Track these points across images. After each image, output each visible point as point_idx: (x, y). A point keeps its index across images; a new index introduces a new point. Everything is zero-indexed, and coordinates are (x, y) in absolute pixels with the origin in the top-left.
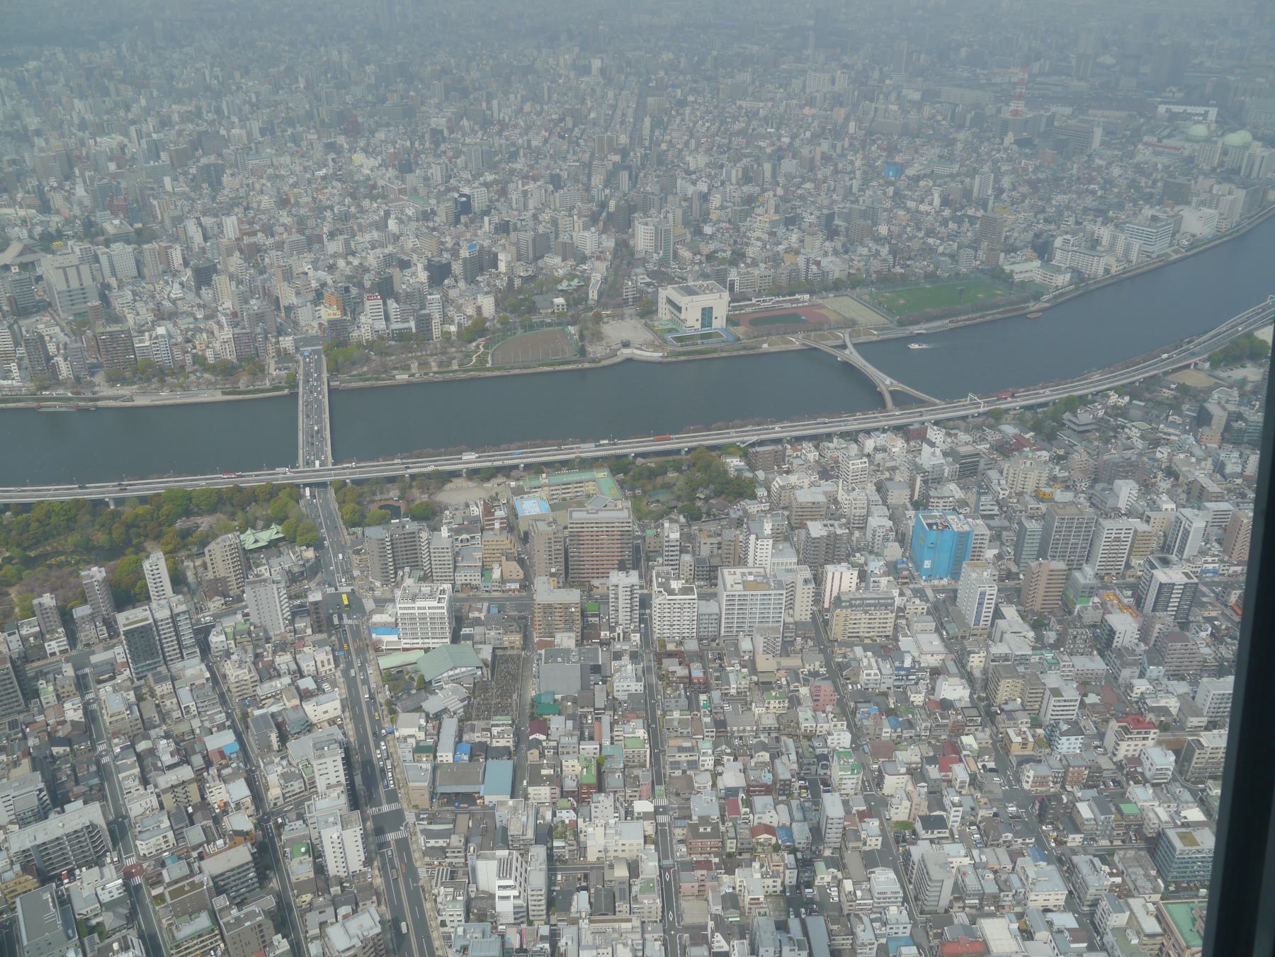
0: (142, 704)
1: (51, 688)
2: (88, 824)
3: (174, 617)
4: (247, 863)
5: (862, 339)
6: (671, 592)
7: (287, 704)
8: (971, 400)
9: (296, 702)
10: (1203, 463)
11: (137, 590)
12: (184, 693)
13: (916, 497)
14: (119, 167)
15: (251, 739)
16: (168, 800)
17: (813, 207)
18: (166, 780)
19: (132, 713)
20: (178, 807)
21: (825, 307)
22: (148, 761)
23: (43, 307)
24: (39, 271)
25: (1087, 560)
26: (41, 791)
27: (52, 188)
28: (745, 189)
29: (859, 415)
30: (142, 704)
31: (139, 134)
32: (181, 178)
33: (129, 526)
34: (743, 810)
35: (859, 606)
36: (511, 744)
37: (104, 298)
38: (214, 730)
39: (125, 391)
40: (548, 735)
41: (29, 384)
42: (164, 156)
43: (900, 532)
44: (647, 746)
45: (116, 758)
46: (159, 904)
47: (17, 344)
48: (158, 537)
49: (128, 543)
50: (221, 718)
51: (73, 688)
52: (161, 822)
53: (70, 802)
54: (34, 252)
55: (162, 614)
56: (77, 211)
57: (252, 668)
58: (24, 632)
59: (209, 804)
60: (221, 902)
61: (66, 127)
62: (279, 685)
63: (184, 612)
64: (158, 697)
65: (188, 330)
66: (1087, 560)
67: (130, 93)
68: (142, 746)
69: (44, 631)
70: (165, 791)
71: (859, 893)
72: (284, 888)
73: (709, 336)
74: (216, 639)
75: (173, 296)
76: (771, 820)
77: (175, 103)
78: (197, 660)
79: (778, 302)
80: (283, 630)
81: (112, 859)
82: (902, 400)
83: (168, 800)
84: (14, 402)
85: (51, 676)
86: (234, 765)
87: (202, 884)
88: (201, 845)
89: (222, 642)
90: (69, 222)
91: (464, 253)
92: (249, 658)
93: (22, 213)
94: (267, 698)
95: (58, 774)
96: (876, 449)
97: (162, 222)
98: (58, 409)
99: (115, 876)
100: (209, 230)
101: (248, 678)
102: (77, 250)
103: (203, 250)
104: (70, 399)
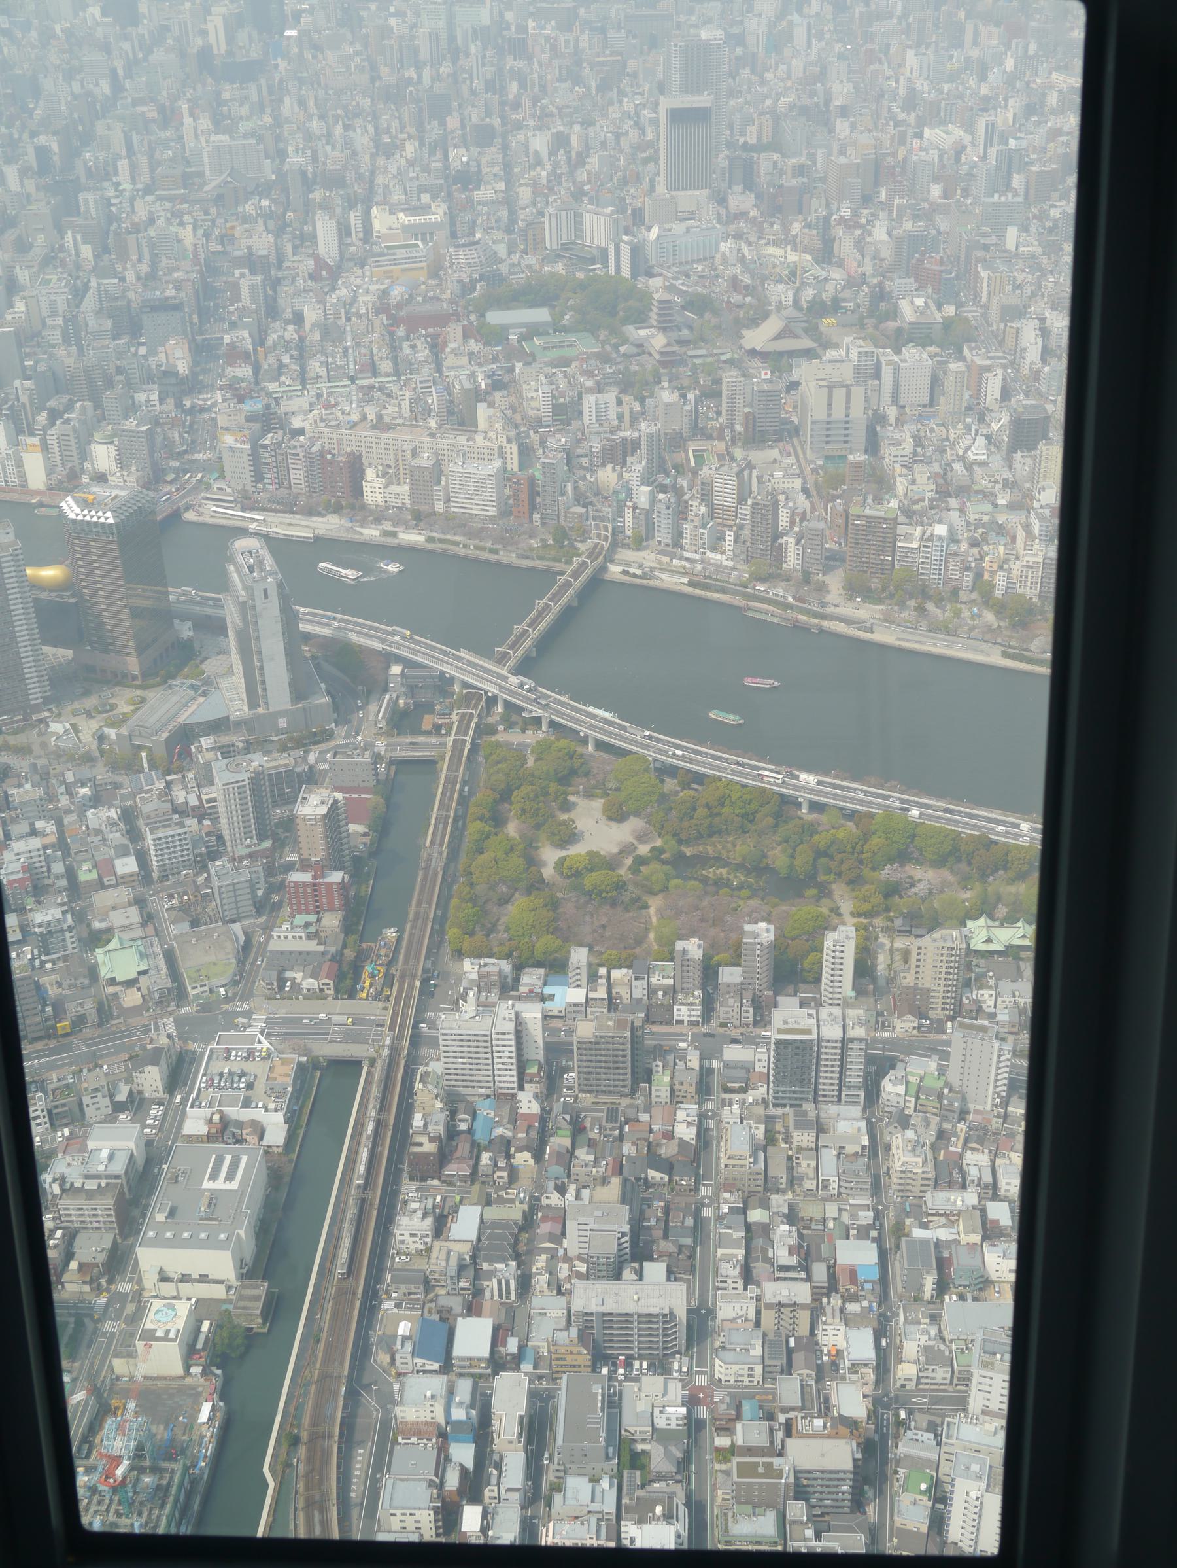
0: (770, 1149)
1: (667, 1079)
2: (667, 1311)
3: (845, 1042)
4: (845, 1472)
7: (962, 1235)
9: (976, 1238)
11: (806, 964)
12: (828, 1157)
14: (946, 195)
15: (897, 1263)
16: (769, 1319)
18: (776, 1292)
19: (755, 1162)
20: (778, 1333)
22: (758, 1242)
23: (786, 433)
24: (795, 375)
26: (623, 1234)
27: (842, 220)
30: (770, 1149)
31: (990, 127)
32: (1034, 226)
33: (820, 853)
37: (873, 445)
38: (853, 1232)
39: (865, 612)
41: (742, 566)
42: (1017, 181)
45: (720, 1218)
46: (719, 1462)
47: (741, 500)
48: (855, 882)
49: (810, 879)
50: (867, 1217)
51: (693, 1089)
52: (753, 1346)
53: (651, 1259)
54: (796, 336)
55: (832, 1032)
56: (868, 268)
57: (930, 1157)
58: (654, 980)
59: (817, 1343)
60: (797, 1510)
61: (885, 103)
62: (959, 1203)
63: (861, 1040)
64: (794, 1146)
65: (979, 524)
67: (994, 42)
68: (756, 1215)
69: (678, 987)
70: (769, 1306)
72: (882, 1524)
74: (892, 1088)
75: (971, 456)
77: (1058, 69)
78: (856, 1111)
80: (988, 1108)
81: (680, 1367)
83: (769, 1319)
84: (717, 591)
85: (670, 1058)
86: (865, 1304)
87: (779, 1474)
88: (793, 1409)
89: (899, 1095)
90: (855, 282)
92: (930, 1136)
93: (793, 257)
94: (937, 1214)
95: (648, 1213)
97: (986, 307)
98: (769, 618)
99: (679, 1401)
100: (1053, 336)
101: (920, 1171)
102: (854, 355)
103: (1036, 376)
104: (790, 607)
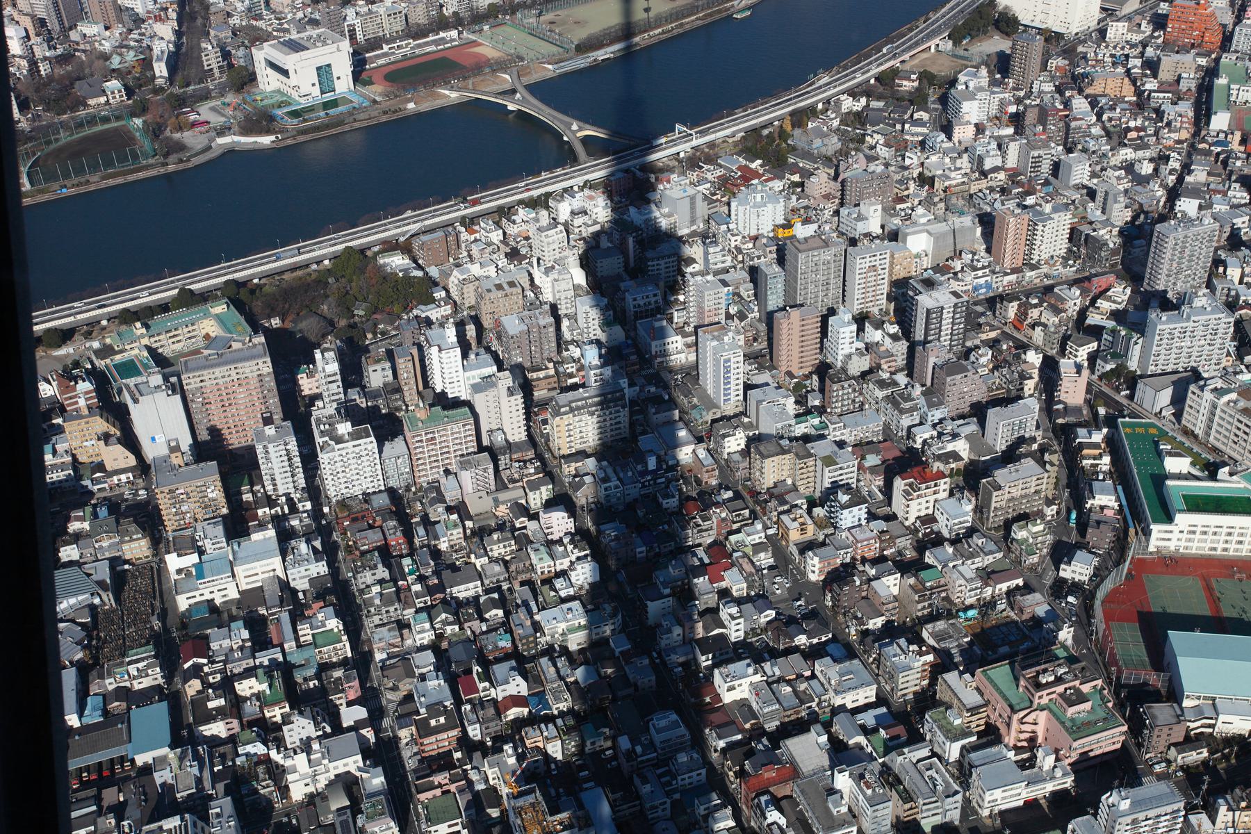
6: (339, 440)
10: (958, 163)
13: (632, 264)
21: (480, 44)
25: (844, 301)
29: (544, 175)
34: (481, 686)
35: (583, 408)
36: (161, 681)
40: (209, 657)
43: (618, 309)
44: (345, 638)
66: (844, 301)
71: (639, 749)
73: (333, 103)
76: (518, 689)
79: (419, 46)
96: (573, 213)
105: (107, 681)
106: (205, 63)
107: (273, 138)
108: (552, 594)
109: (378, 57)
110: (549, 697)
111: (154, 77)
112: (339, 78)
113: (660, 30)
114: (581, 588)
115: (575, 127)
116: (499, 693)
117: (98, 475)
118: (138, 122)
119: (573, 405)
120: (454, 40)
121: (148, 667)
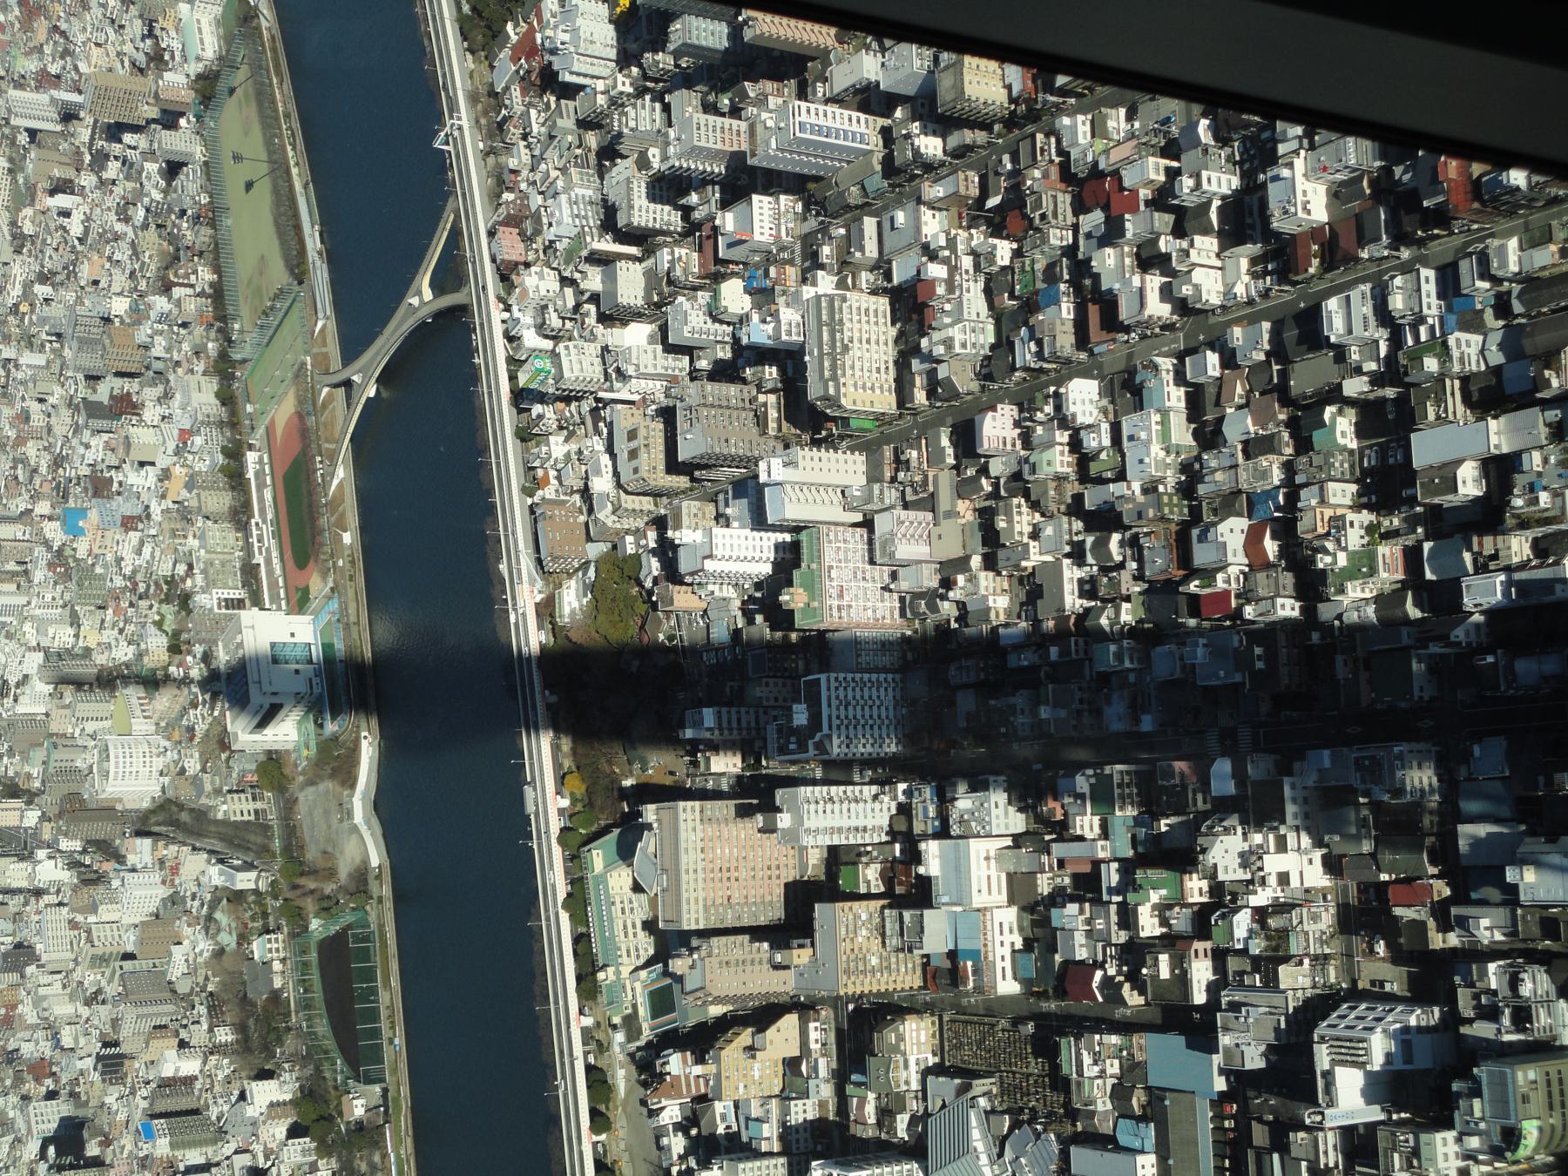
5: (333, 349)
8: (447, 143)
17: (75, 442)
28: (39, 575)
35: (834, 361)
82: (451, 274)
91: (162, 1147)
105: (1100, 1107)
106: (246, 818)
107: (364, 744)
108: (1103, 456)
109: (270, 572)
110: (1260, 487)
111: (256, 892)
112: (293, 635)
113: (289, 148)
114: (1104, 411)
115: (415, 301)
116: (1237, 561)
117: (804, 1068)
118: (315, 924)
119: (827, 374)
120: (261, 459)
121: (1090, 1050)
